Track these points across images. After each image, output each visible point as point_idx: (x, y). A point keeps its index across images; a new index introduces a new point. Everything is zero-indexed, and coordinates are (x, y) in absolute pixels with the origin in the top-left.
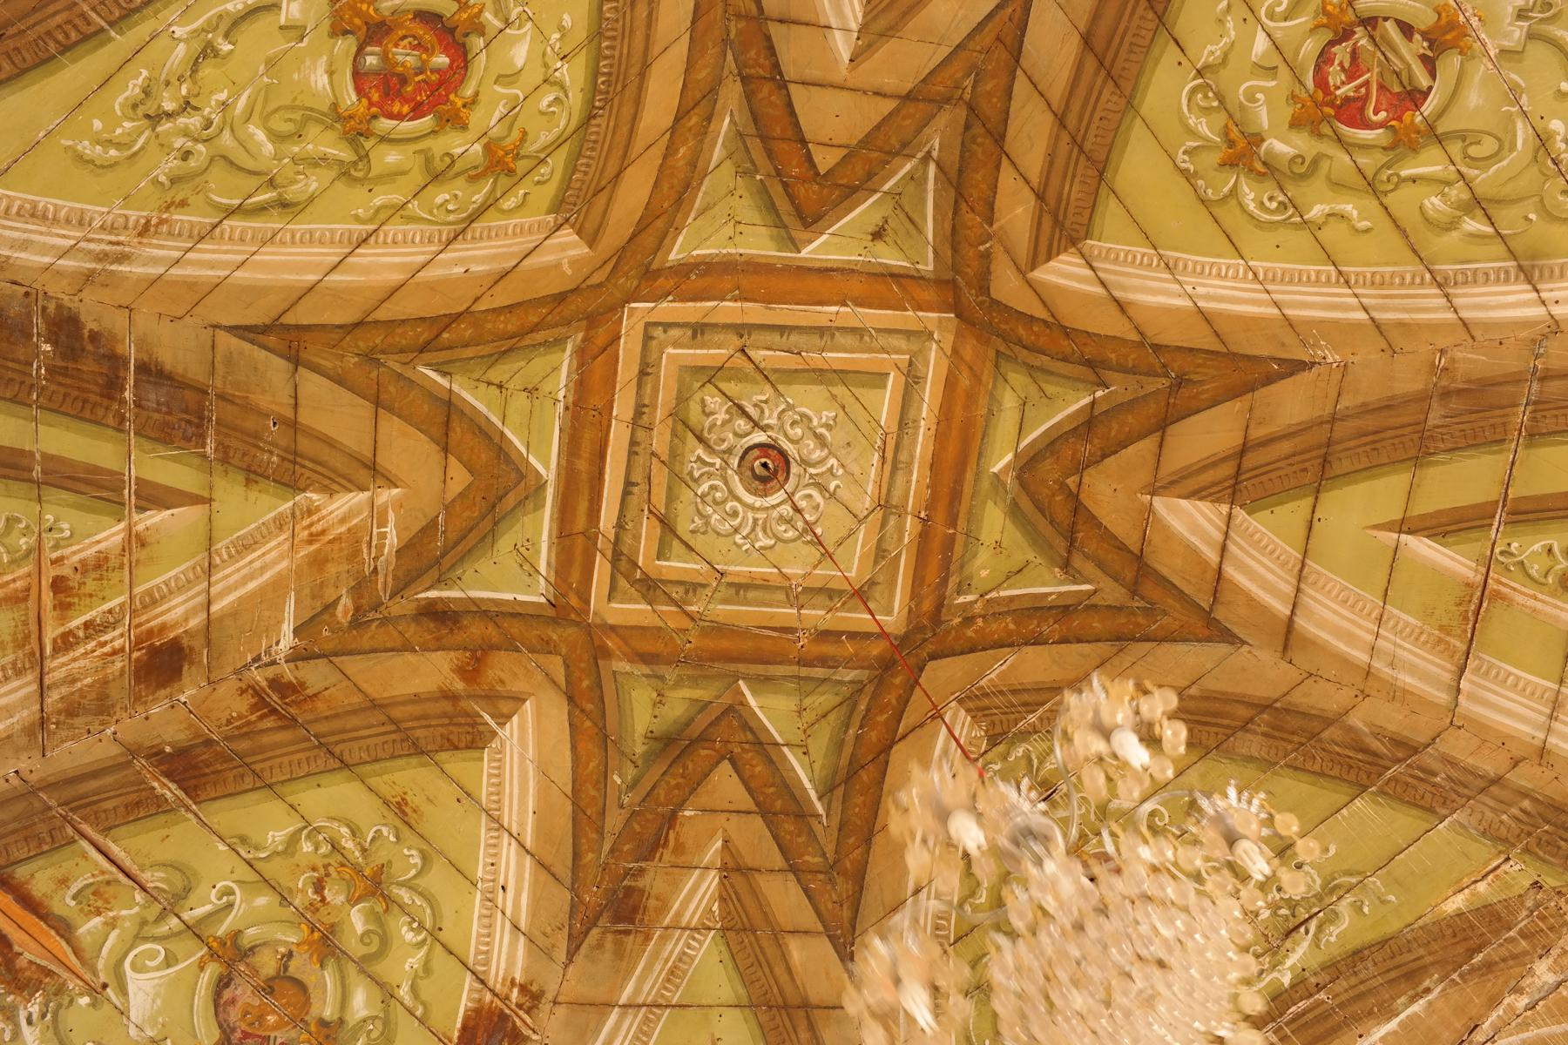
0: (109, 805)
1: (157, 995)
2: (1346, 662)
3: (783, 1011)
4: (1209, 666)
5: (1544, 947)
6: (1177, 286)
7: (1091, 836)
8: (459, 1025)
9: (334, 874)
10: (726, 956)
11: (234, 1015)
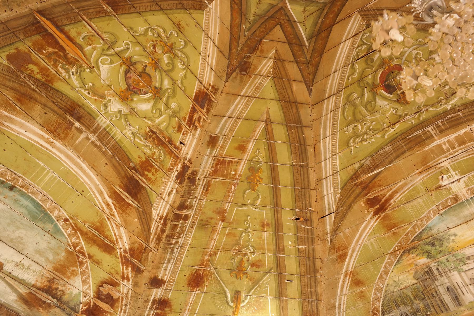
0: (91, 11)
1: (108, 72)
3: (289, 103)
7: (395, 59)
8: (194, 95)
9: (159, 44)
10: (273, 85)
11: (131, 81)
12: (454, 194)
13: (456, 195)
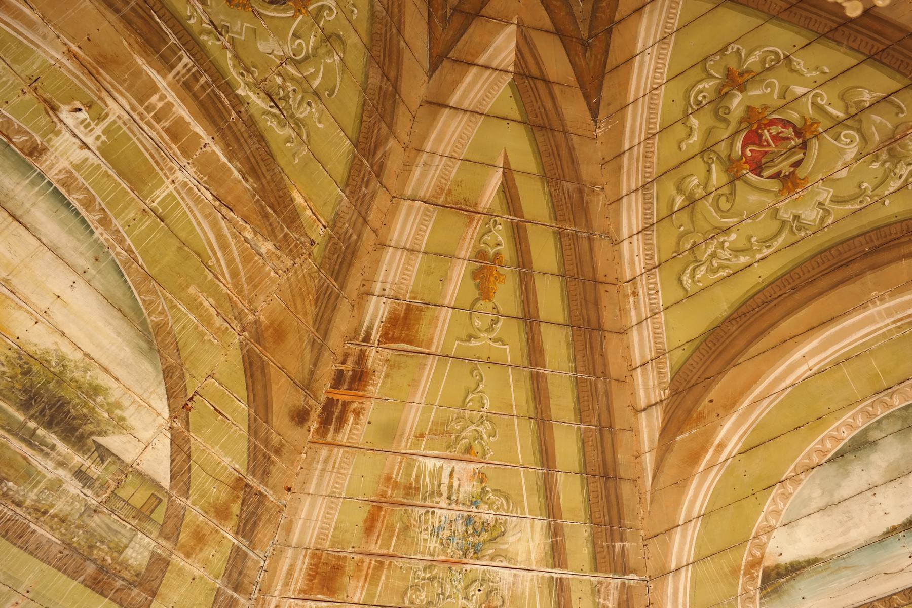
2: (424, 138)
4: (416, 54)
5: (280, 247)
6: (651, 43)
12: (46, 144)
13: (44, 150)
